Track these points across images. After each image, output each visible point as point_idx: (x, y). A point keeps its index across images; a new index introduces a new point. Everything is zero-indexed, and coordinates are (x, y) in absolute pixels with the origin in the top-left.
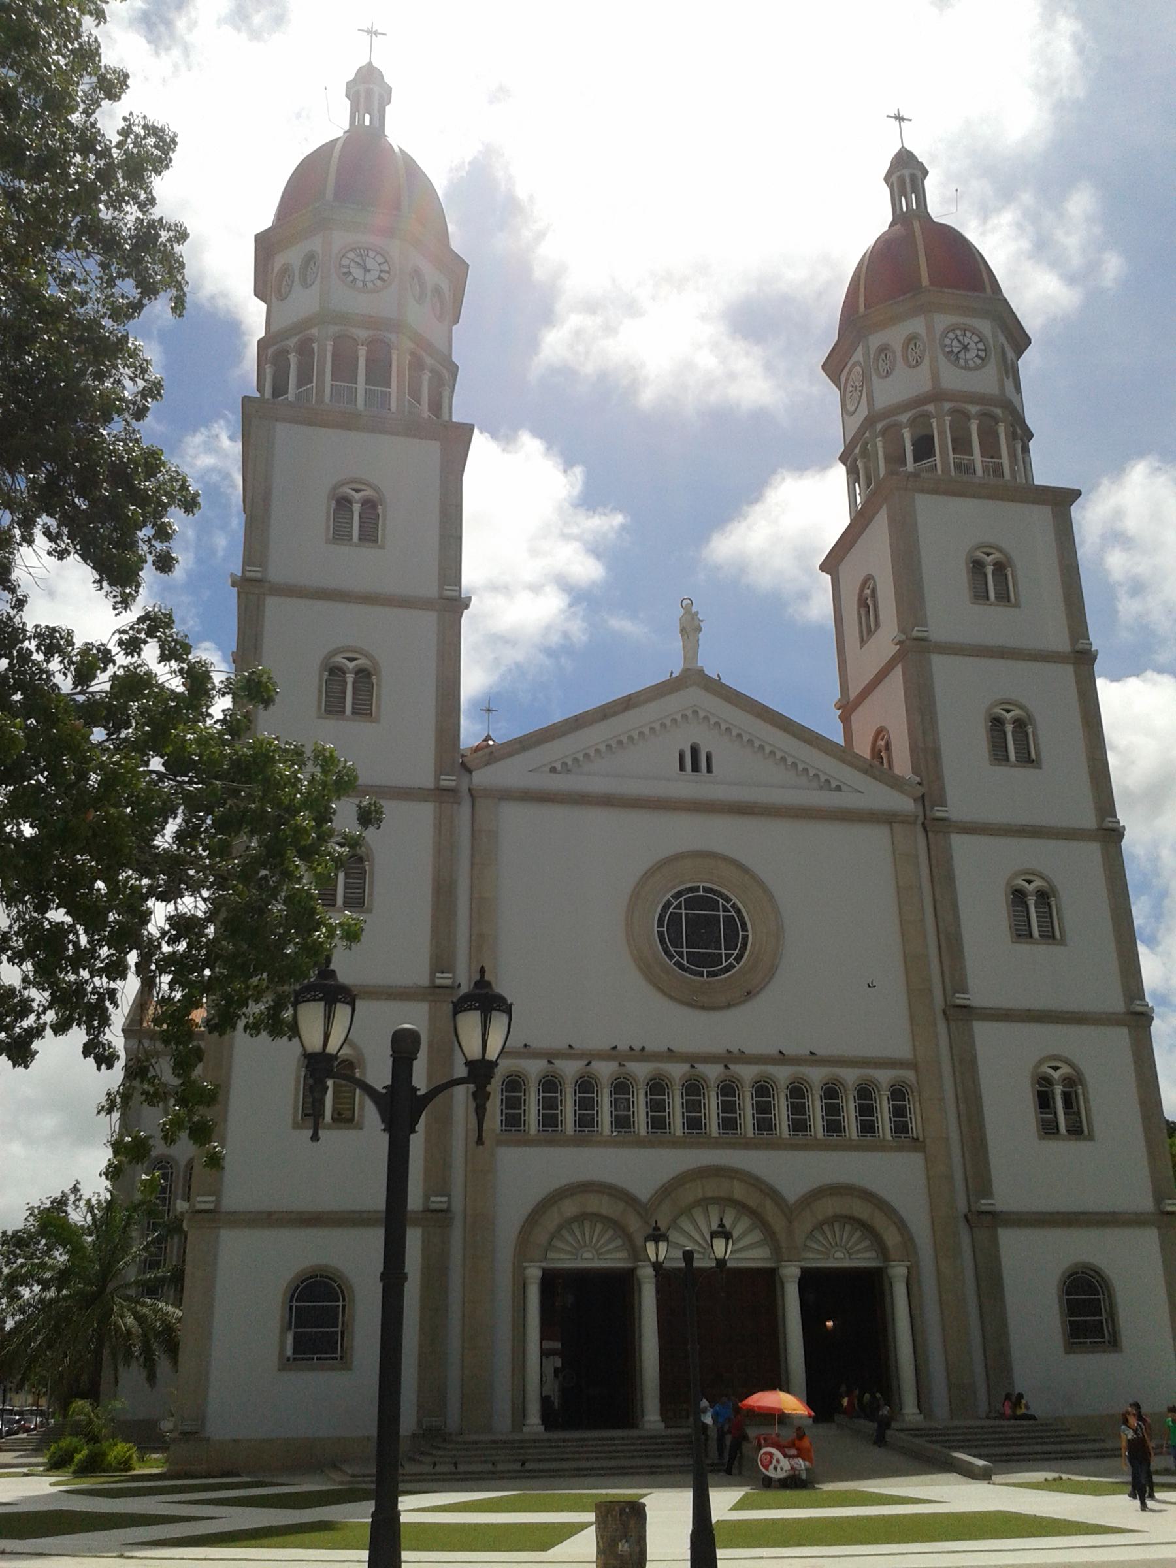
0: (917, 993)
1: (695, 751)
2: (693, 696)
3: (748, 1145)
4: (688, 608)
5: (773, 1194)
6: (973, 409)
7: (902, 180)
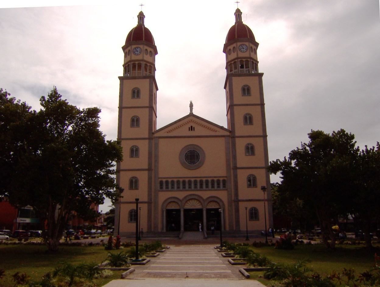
0: (228, 165)
1: (192, 127)
2: (191, 118)
3: (198, 190)
4: (191, 103)
5: (201, 198)
6: (244, 60)
7: (237, 15)
